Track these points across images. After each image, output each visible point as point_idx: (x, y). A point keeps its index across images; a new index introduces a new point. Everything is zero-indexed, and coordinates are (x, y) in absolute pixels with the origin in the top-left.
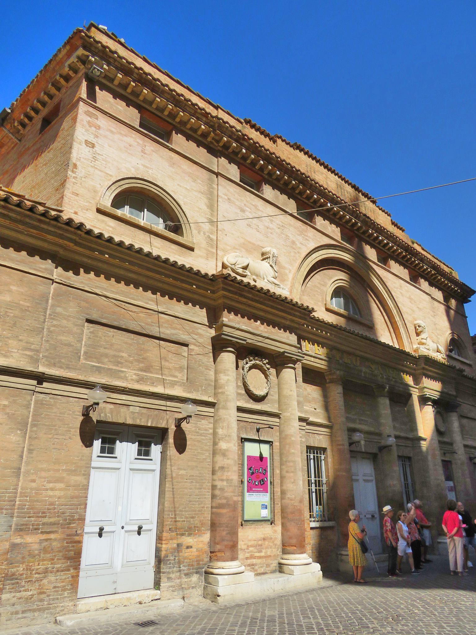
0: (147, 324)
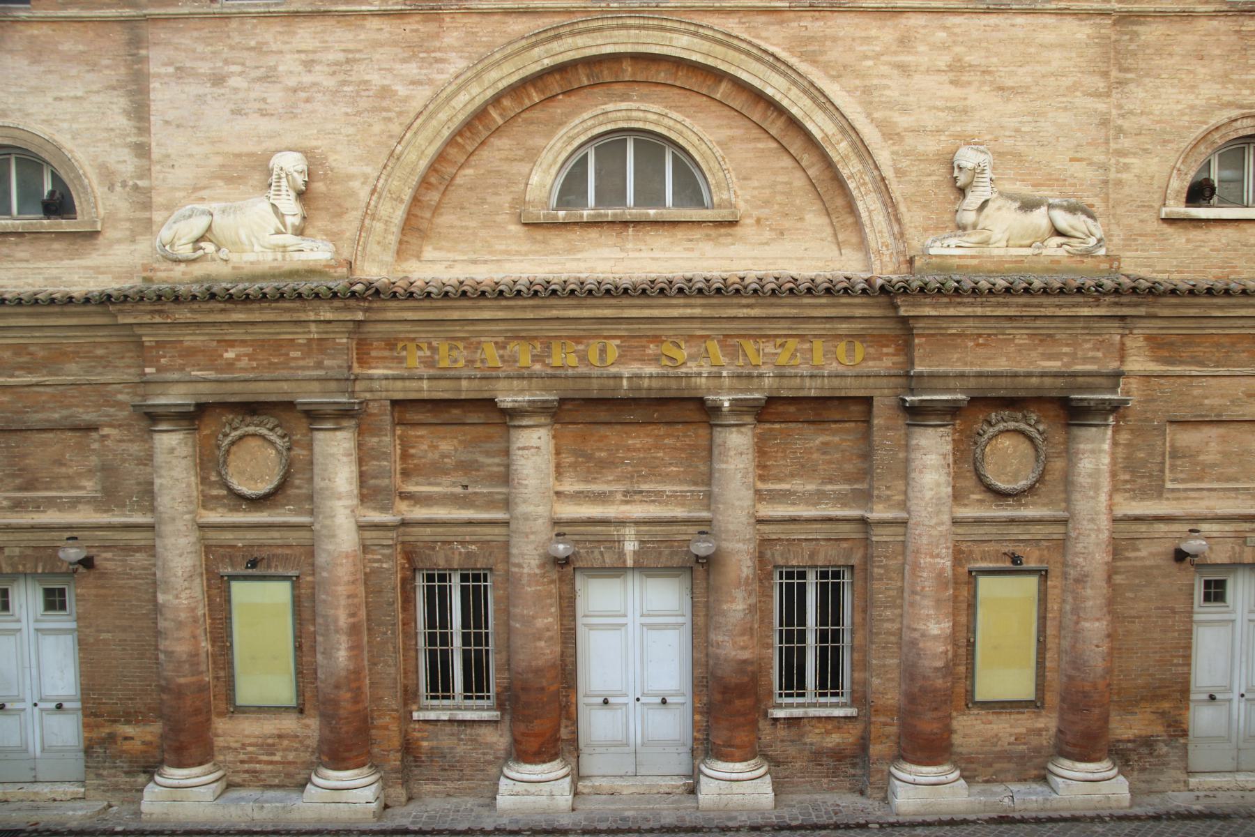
0: (16, 412)
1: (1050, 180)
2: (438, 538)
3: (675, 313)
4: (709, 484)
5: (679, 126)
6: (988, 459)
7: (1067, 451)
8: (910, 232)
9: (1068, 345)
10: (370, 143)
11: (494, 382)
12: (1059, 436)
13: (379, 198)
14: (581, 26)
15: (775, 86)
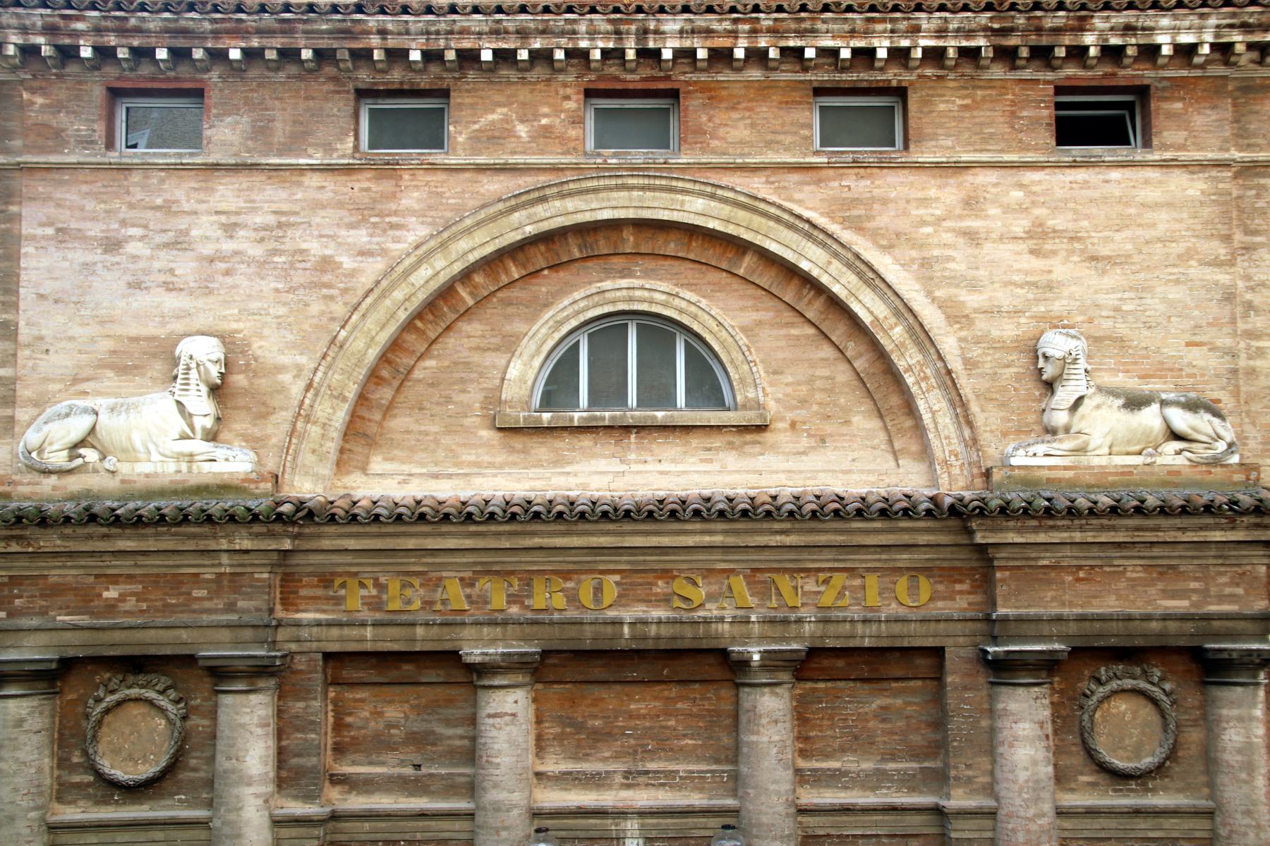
1: (1161, 371)
2: (379, 836)
3: (690, 541)
4: (735, 761)
5: (693, 309)
6: (1100, 728)
7: (1205, 717)
8: (985, 437)
9: (1196, 579)
10: (306, 327)
11: (458, 629)
12: (1192, 699)
13: (316, 395)
14: (572, 186)
15: (811, 259)
